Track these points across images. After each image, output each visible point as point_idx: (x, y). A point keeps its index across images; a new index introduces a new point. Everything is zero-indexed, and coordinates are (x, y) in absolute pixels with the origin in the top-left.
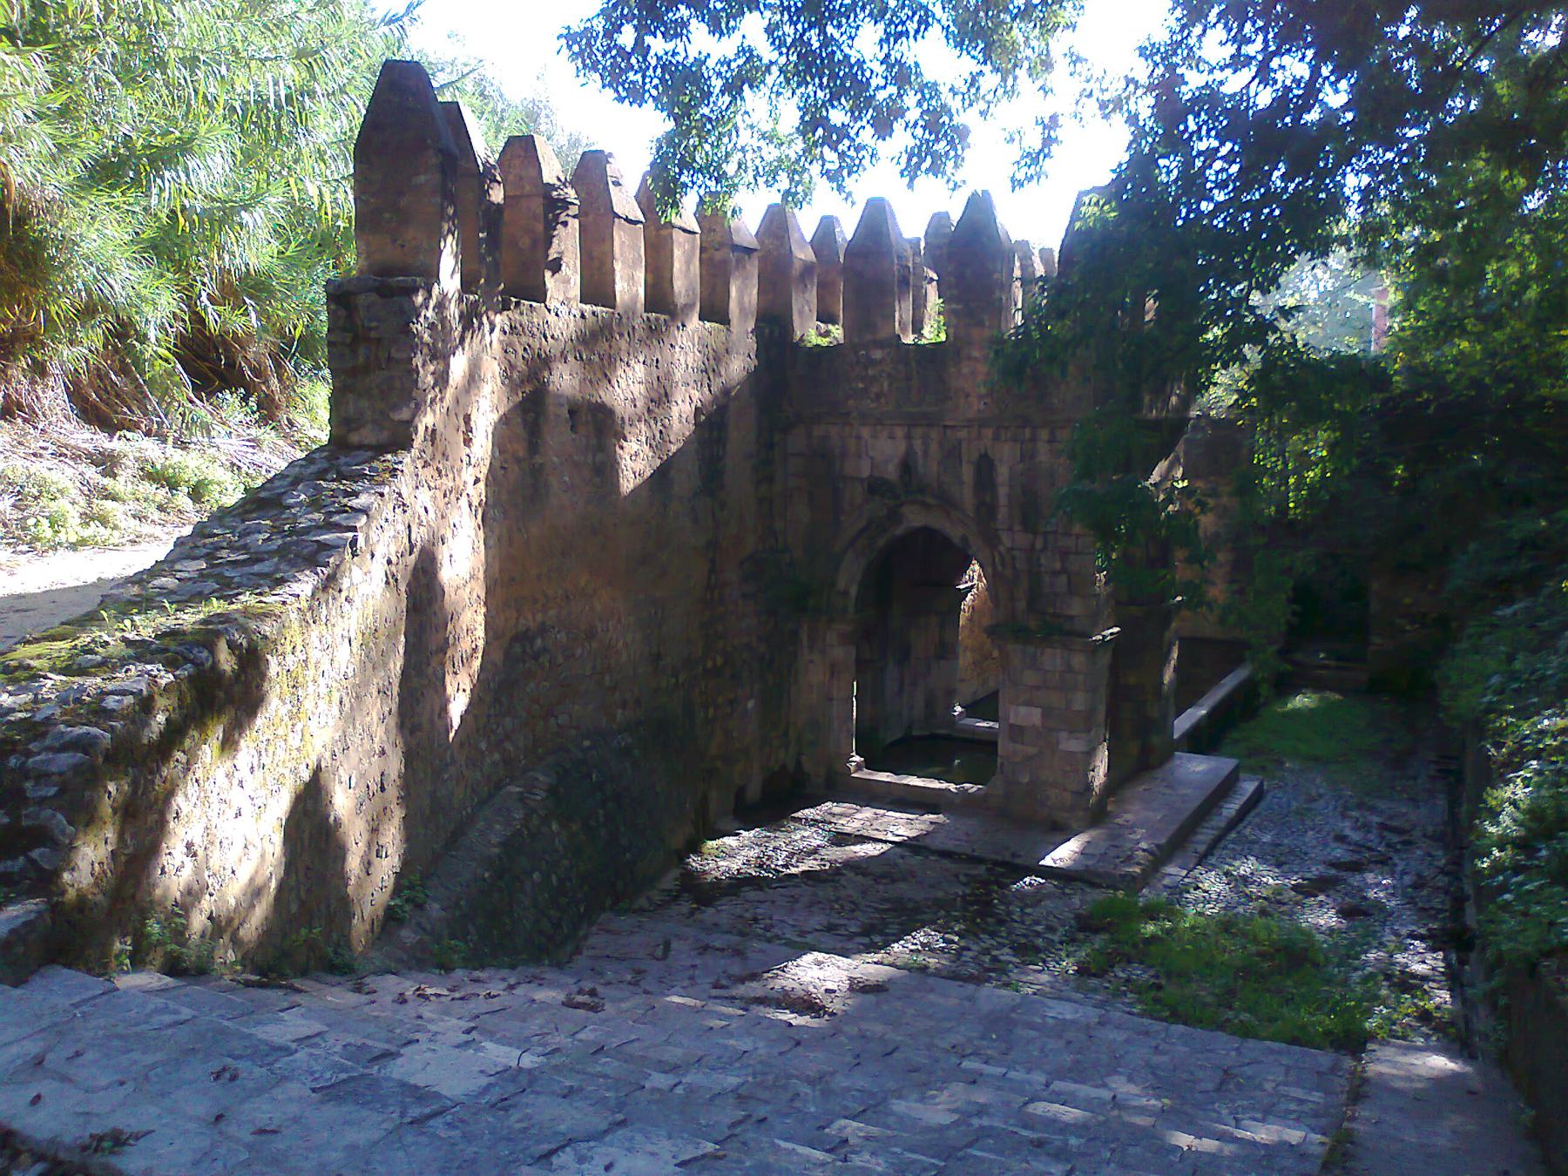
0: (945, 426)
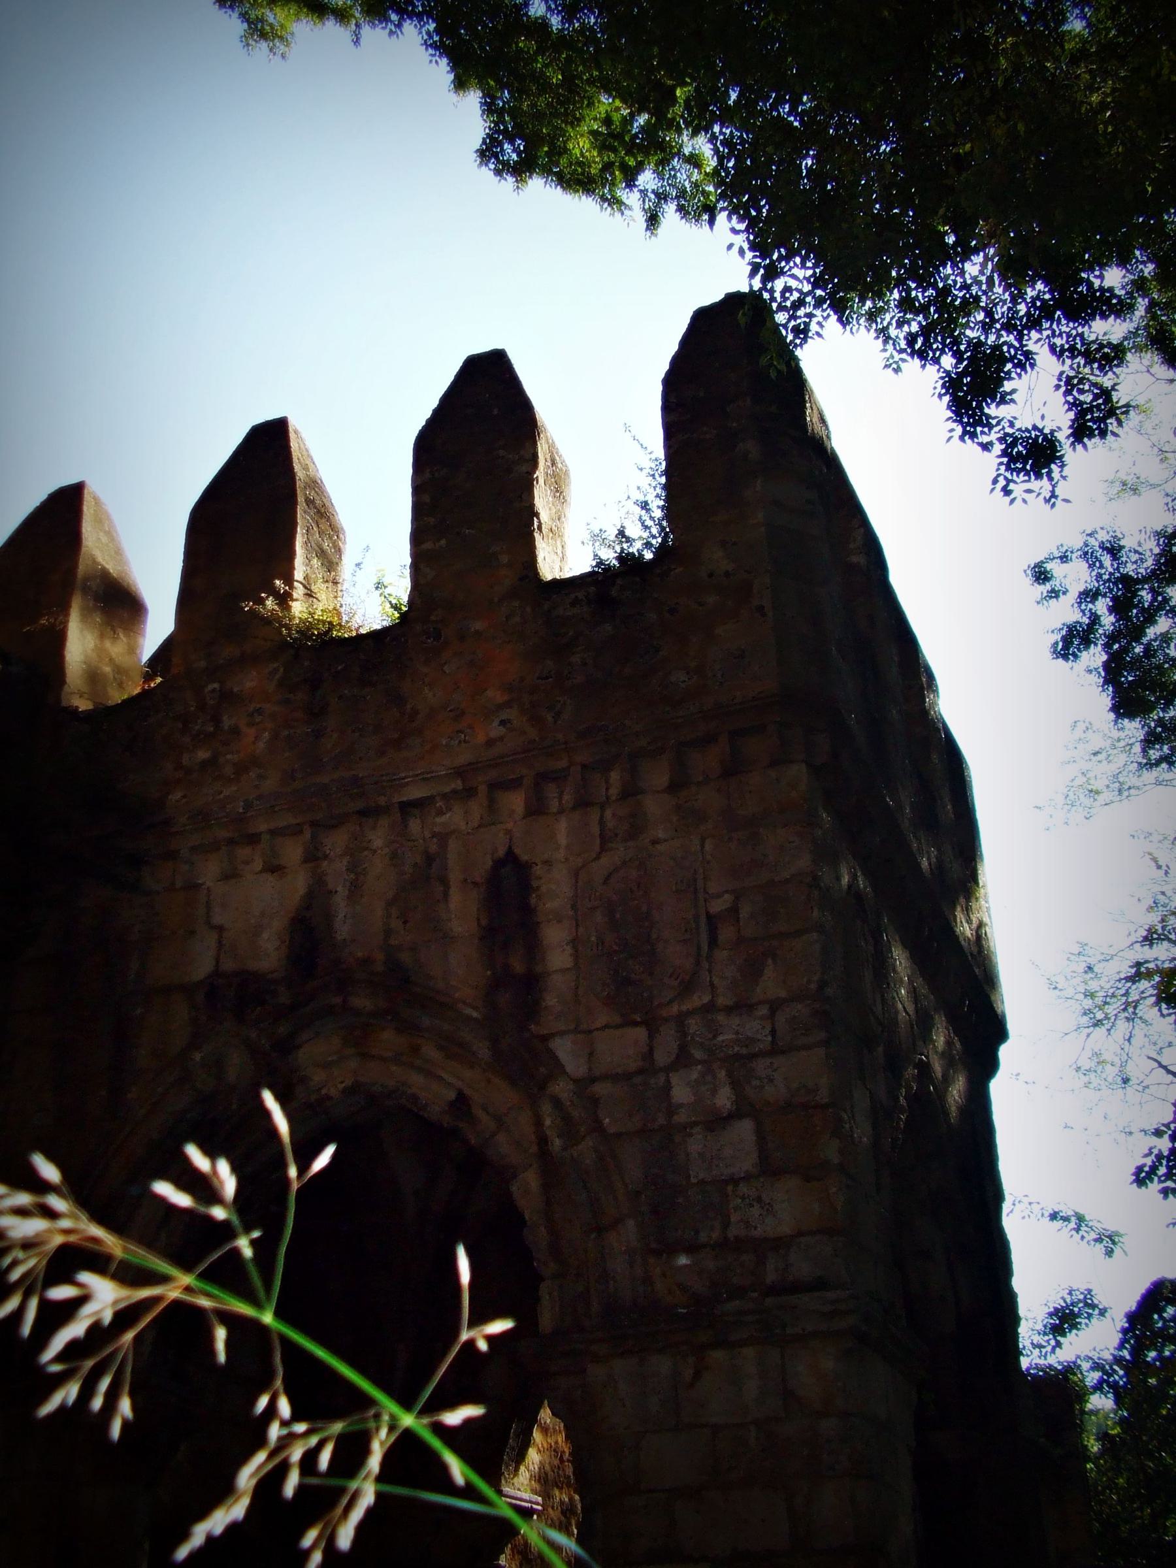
0: (406, 808)
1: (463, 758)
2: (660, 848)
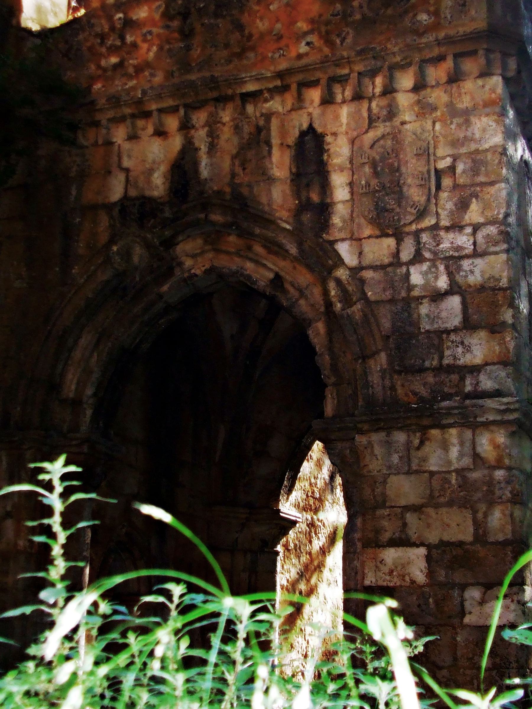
1: (283, 65)
2: (407, 127)
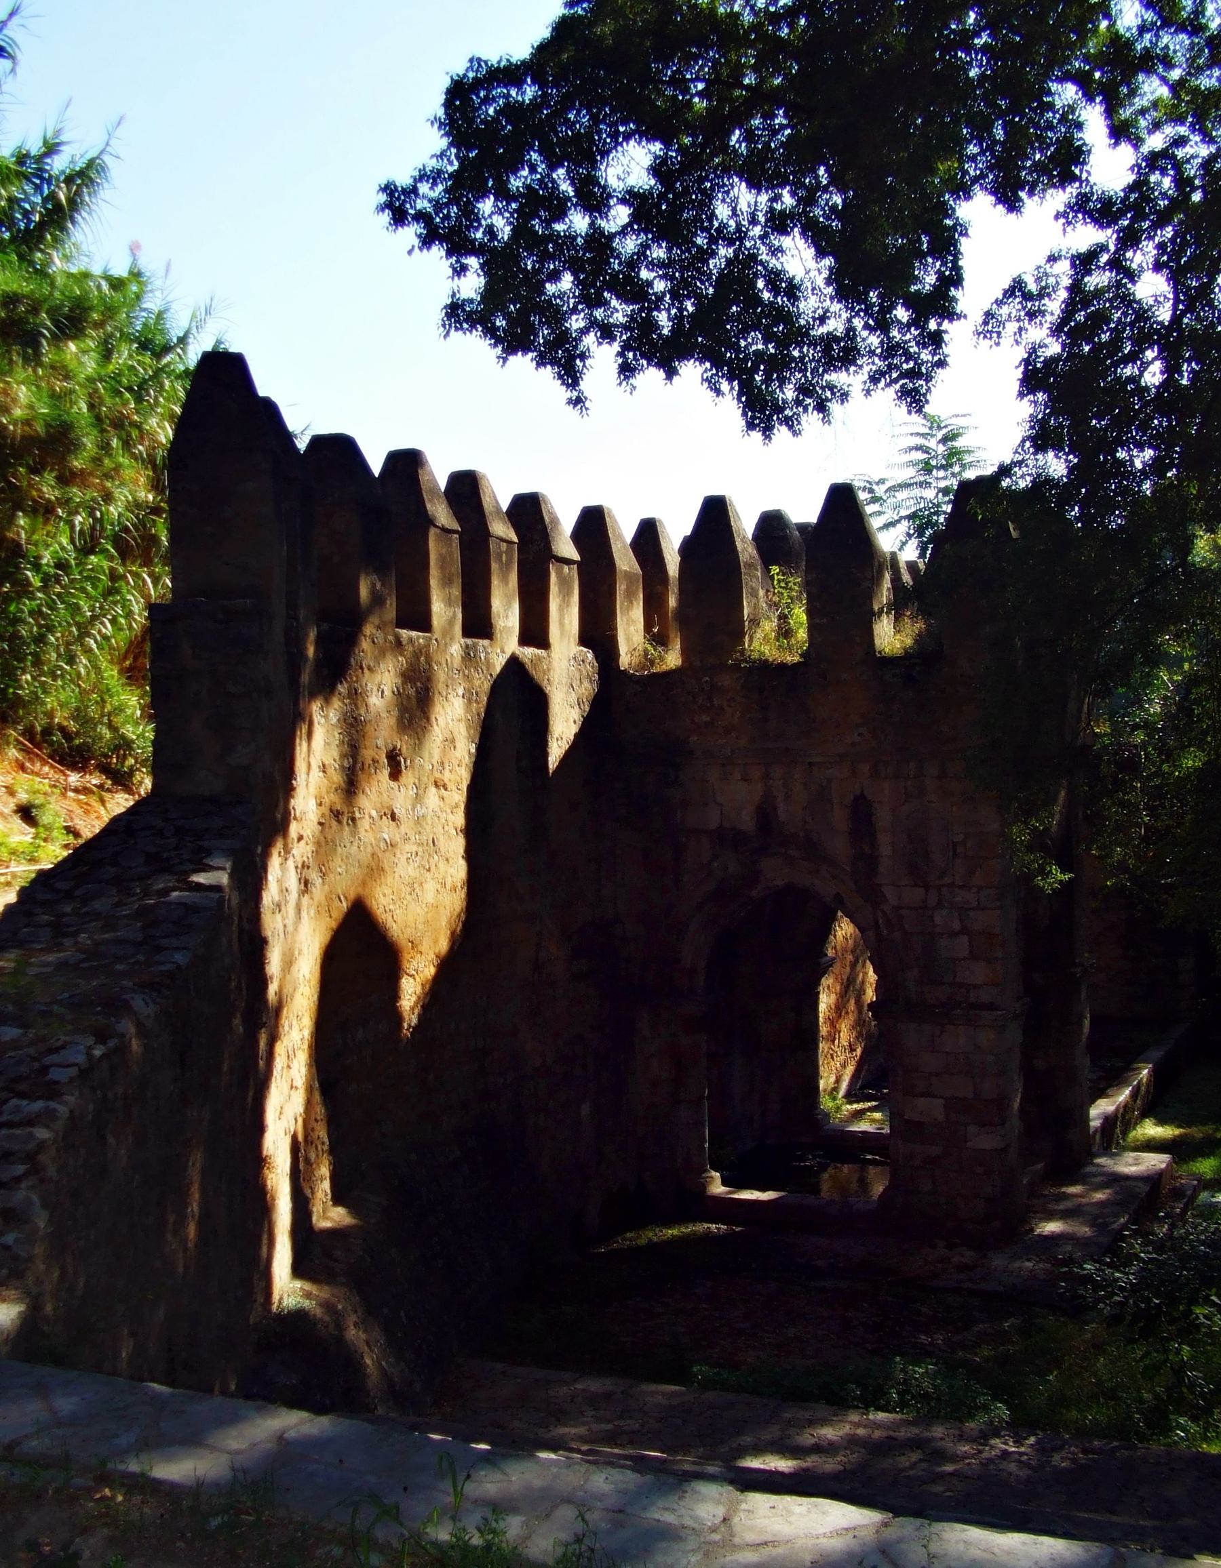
0: (810, 764)
